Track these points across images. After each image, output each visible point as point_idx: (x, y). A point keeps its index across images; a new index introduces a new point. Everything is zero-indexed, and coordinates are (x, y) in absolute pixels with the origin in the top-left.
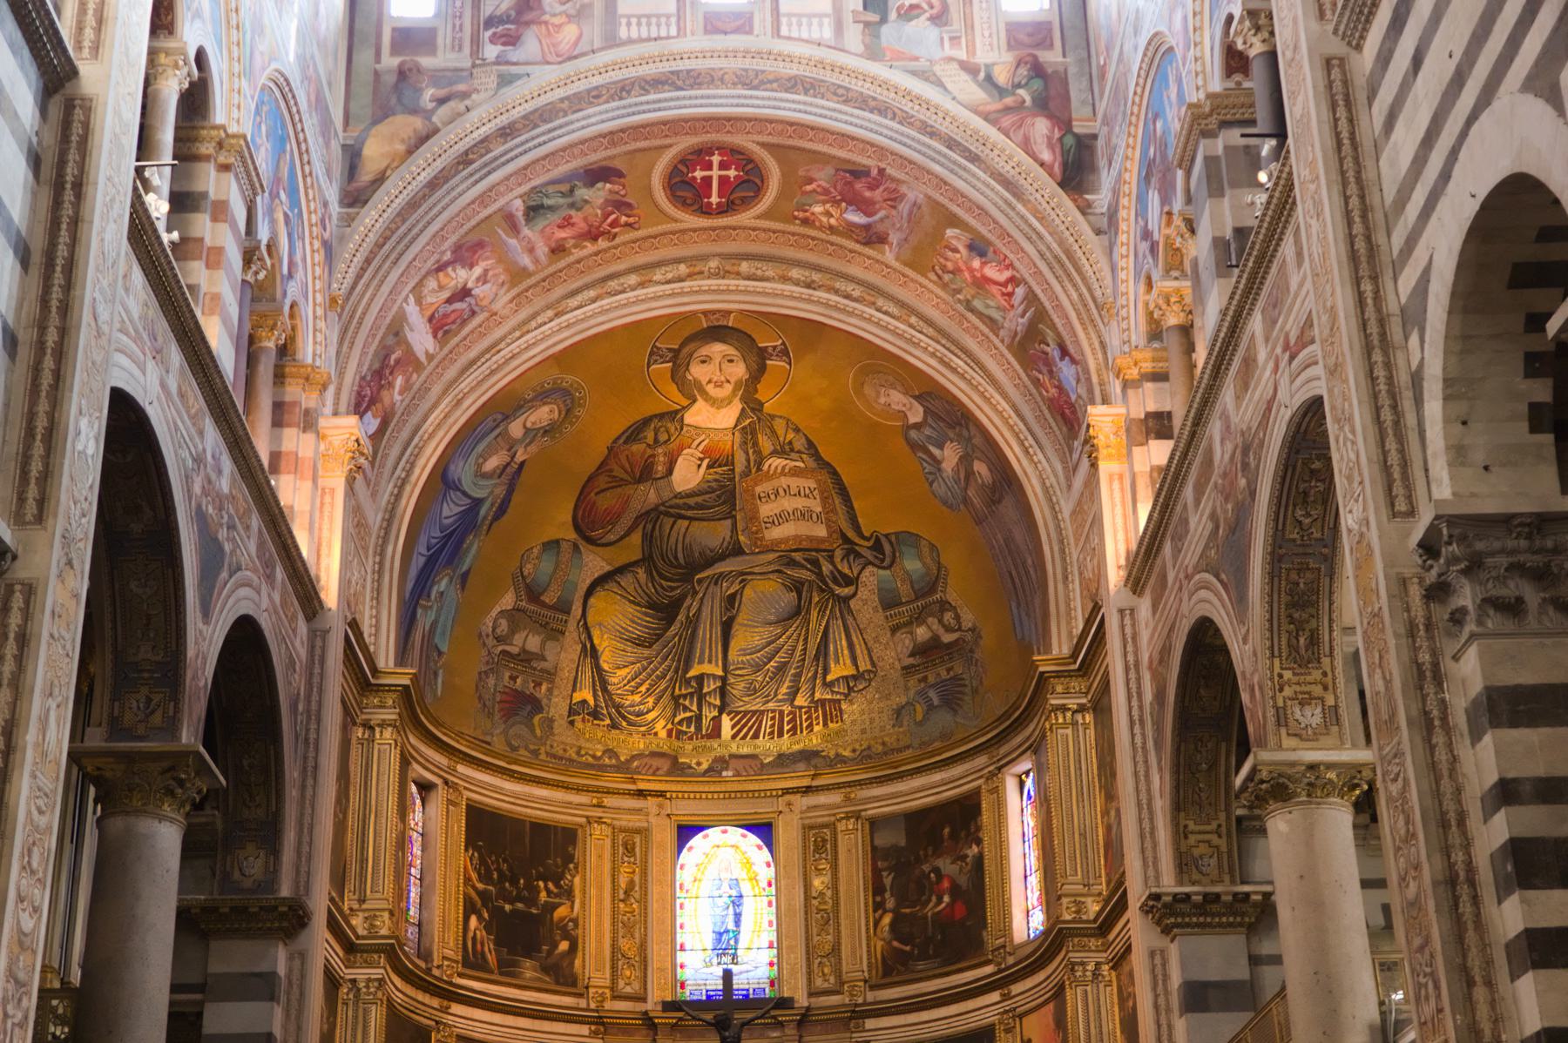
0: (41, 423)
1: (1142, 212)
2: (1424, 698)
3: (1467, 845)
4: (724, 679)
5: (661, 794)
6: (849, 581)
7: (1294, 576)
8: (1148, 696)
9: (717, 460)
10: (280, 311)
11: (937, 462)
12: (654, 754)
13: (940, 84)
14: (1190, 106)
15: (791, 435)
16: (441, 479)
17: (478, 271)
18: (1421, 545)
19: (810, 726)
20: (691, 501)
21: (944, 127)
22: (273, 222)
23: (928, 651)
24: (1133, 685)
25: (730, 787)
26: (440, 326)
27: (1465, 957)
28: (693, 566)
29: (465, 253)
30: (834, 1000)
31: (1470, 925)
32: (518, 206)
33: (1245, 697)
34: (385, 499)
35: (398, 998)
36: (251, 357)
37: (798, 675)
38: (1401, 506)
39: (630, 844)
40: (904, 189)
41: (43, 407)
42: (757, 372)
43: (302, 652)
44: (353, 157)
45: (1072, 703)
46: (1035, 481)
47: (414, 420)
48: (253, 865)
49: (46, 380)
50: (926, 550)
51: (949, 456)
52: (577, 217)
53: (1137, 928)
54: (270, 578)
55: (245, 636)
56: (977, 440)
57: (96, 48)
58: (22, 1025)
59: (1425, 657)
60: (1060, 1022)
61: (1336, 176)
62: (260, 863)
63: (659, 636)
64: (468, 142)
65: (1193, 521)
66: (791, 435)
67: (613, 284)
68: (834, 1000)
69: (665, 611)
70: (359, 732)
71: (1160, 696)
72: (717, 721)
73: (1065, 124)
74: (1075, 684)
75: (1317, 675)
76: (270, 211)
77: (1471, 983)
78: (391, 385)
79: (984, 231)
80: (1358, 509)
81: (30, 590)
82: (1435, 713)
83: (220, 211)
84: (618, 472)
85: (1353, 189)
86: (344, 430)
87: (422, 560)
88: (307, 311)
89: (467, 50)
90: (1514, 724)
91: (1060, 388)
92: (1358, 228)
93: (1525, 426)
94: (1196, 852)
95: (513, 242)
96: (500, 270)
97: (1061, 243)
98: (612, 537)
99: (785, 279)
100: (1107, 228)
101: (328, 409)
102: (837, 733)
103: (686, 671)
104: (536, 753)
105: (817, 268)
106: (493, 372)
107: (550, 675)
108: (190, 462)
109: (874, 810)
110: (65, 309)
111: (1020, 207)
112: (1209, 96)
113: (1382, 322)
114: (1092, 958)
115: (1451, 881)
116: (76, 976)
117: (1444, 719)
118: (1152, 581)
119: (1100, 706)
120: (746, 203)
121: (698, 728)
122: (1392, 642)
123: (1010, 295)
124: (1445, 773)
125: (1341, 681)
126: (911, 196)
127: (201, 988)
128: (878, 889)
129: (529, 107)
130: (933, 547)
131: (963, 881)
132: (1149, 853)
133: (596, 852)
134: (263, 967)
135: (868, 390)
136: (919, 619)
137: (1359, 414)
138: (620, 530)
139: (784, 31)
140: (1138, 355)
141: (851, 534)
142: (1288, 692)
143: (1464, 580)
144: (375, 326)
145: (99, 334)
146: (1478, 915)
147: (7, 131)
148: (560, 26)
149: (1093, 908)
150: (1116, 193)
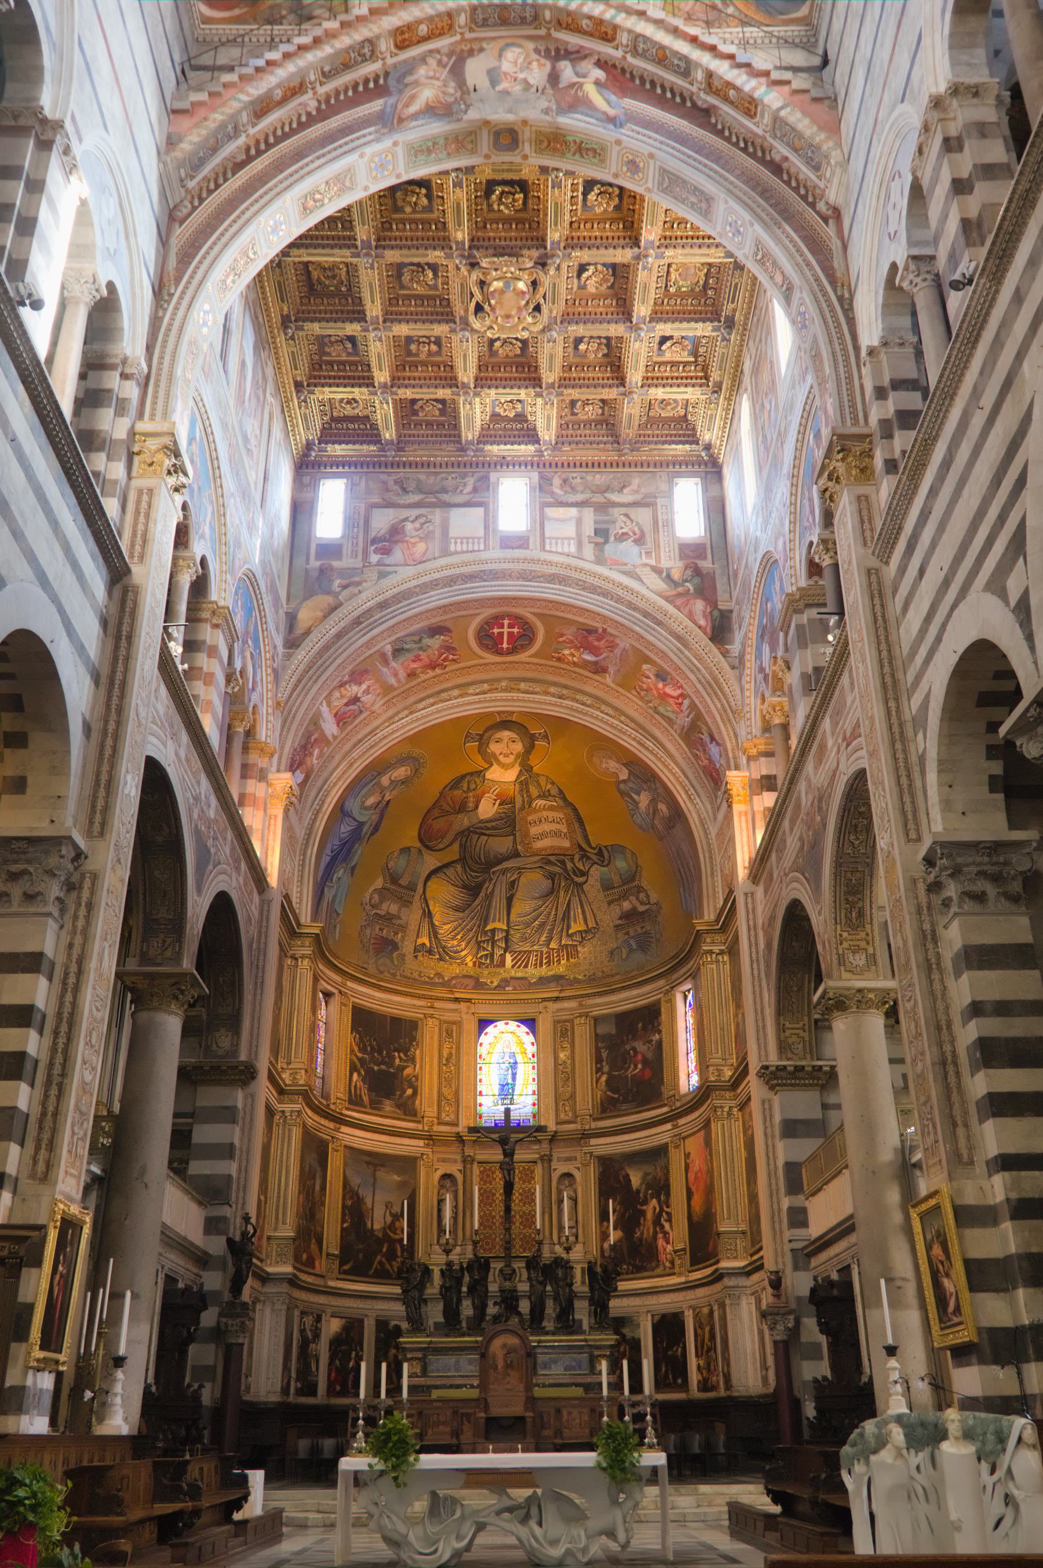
0: (104, 777)
1: (759, 655)
2: (926, 951)
3: (953, 1042)
4: (507, 932)
5: (469, 1000)
6: (583, 874)
7: (849, 875)
8: (762, 945)
9: (505, 800)
10: (246, 710)
11: (636, 803)
12: (465, 976)
13: (639, 579)
14: (788, 595)
15: (549, 786)
16: (341, 811)
17: (364, 687)
18: (924, 859)
19: (559, 961)
20: (489, 825)
21: (642, 605)
22: (244, 658)
23: (630, 916)
24: (753, 939)
25: (510, 997)
26: (341, 719)
27: (951, 1109)
28: (490, 864)
29: (357, 676)
30: (572, 1127)
31: (955, 1090)
32: (388, 649)
33: (819, 947)
34: (306, 821)
35: (309, 1122)
36: (229, 738)
37: (551, 930)
38: (913, 835)
39: (450, 1031)
40: (618, 641)
41: (105, 768)
42: (529, 749)
43: (255, 912)
44: (292, 619)
45: (716, 949)
46: (695, 815)
47: (325, 774)
48: (223, 1040)
49: (108, 751)
50: (629, 856)
51: (644, 800)
52: (423, 655)
53: (754, 1085)
54: (237, 869)
55: (222, 905)
56: (660, 790)
57: (142, 557)
58: (83, 1139)
59: (927, 926)
60: (708, 1142)
61: (873, 639)
62: (229, 1039)
63: (469, 906)
64: (360, 611)
66: (549, 786)
67: (444, 695)
68: (572, 1127)
69: (473, 890)
70: (289, 961)
71: (769, 945)
72: (503, 957)
74: (718, 938)
75: (863, 935)
76: (242, 652)
77: (955, 1125)
78: (311, 754)
79: (665, 666)
80: (887, 836)
81: (95, 877)
82: (933, 960)
83: (213, 652)
84: (447, 808)
85: (883, 646)
86: (283, 781)
87: (328, 859)
88: (263, 710)
89: (360, 557)
90: (981, 967)
91: (710, 760)
92: (887, 669)
93: (987, 788)
94: (790, 1041)
95: (385, 670)
96: (377, 686)
97: (711, 673)
98: (441, 846)
99: (546, 693)
100: (738, 665)
101: (274, 769)
102: (575, 965)
103: (485, 926)
104: (394, 975)
105: (566, 687)
106: (372, 747)
107: (403, 928)
108: (191, 800)
110: (120, 710)
111: (686, 652)
112: (798, 589)
113: (901, 725)
114: (727, 1104)
115: (943, 1063)
116: (117, 1108)
117: (938, 964)
118: (764, 876)
119: (733, 951)
120: (524, 648)
121: (492, 960)
122: (907, 917)
123: (681, 704)
124: (939, 996)
125: (877, 938)
126: (622, 645)
127: (191, 1115)
128: (599, 1060)
129: (396, 591)
130: (633, 853)
131: (650, 1055)
132: (762, 1041)
133: (429, 1036)
134: (228, 1103)
135: (595, 759)
136: (624, 896)
137: (888, 780)
138: (446, 842)
139: (547, 548)
140: (756, 741)
141: (584, 846)
142: (845, 945)
143: (950, 880)
144: (302, 719)
145: (140, 725)
146: (959, 1083)
147: (89, 607)
148: (415, 544)
149: (728, 1073)
150: (744, 645)
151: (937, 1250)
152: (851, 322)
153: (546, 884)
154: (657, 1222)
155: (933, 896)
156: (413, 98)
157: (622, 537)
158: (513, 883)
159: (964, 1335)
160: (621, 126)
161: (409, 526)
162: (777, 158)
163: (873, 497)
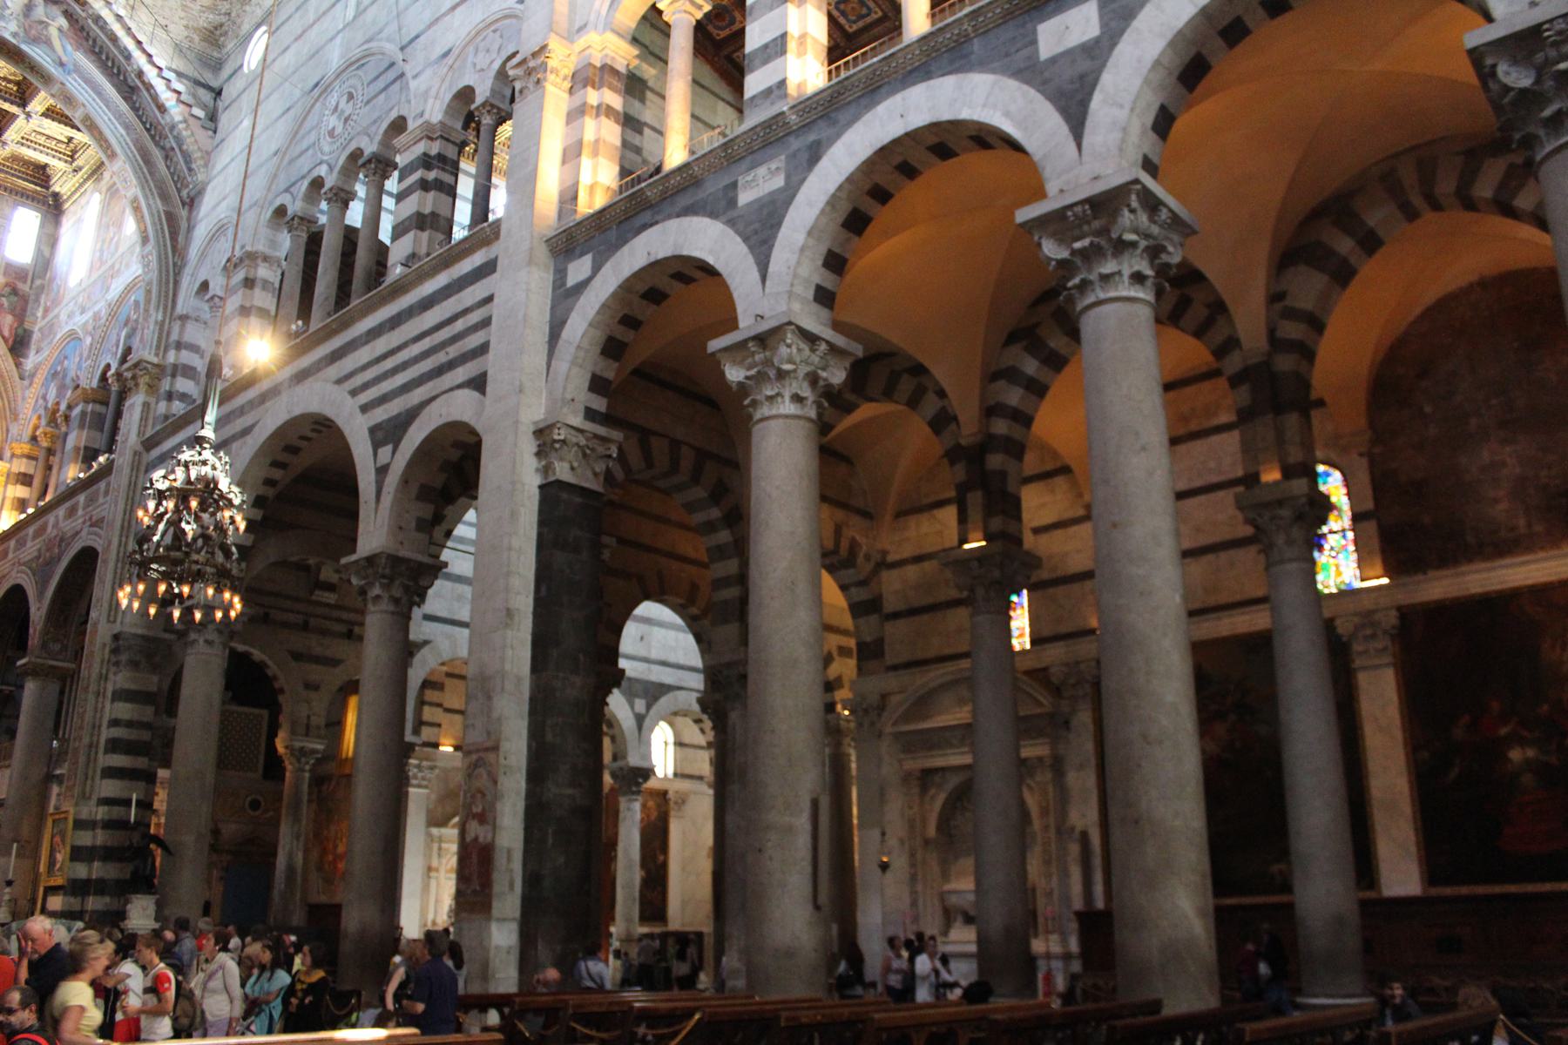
3: (99, 735)
33: (31, 631)
59: (104, 671)
65: (29, 544)
77: (87, 778)
82: (102, 690)
115: (90, 746)
150: (36, 368)
151: (58, 839)
152: (176, 283)
155: (112, 656)
159: (59, 881)
160: (69, 73)
162: (168, 146)
163: (153, 406)
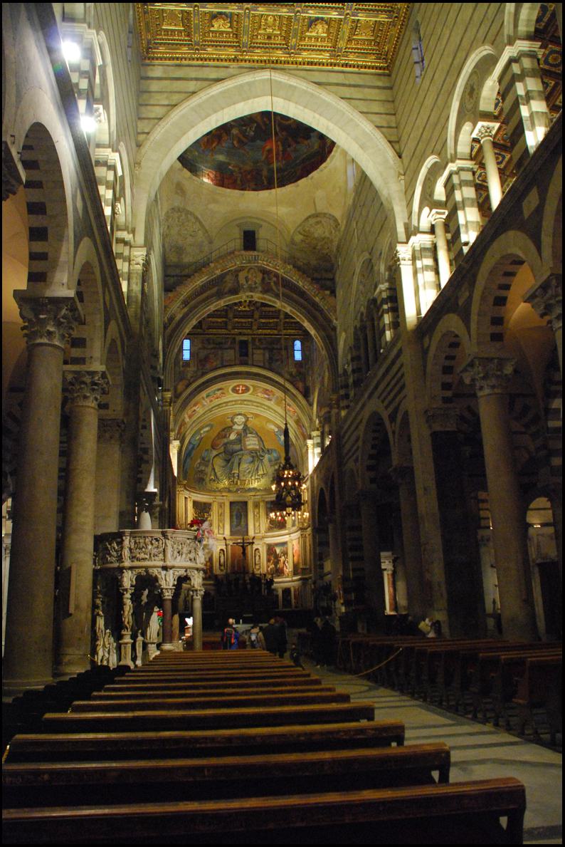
6: (262, 456)
12: (226, 488)
29: (195, 405)
69: (228, 461)
72: (237, 482)
73: (305, 384)
95: (203, 401)
99: (253, 405)
107: (206, 474)
109: (267, 500)
133: (215, 507)
148: (212, 363)
152: (337, 362)
153: (252, 459)
154: (284, 563)
156: (225, 287)
157: (277, 360)
158: (240, 459)
161: (211, 356)
